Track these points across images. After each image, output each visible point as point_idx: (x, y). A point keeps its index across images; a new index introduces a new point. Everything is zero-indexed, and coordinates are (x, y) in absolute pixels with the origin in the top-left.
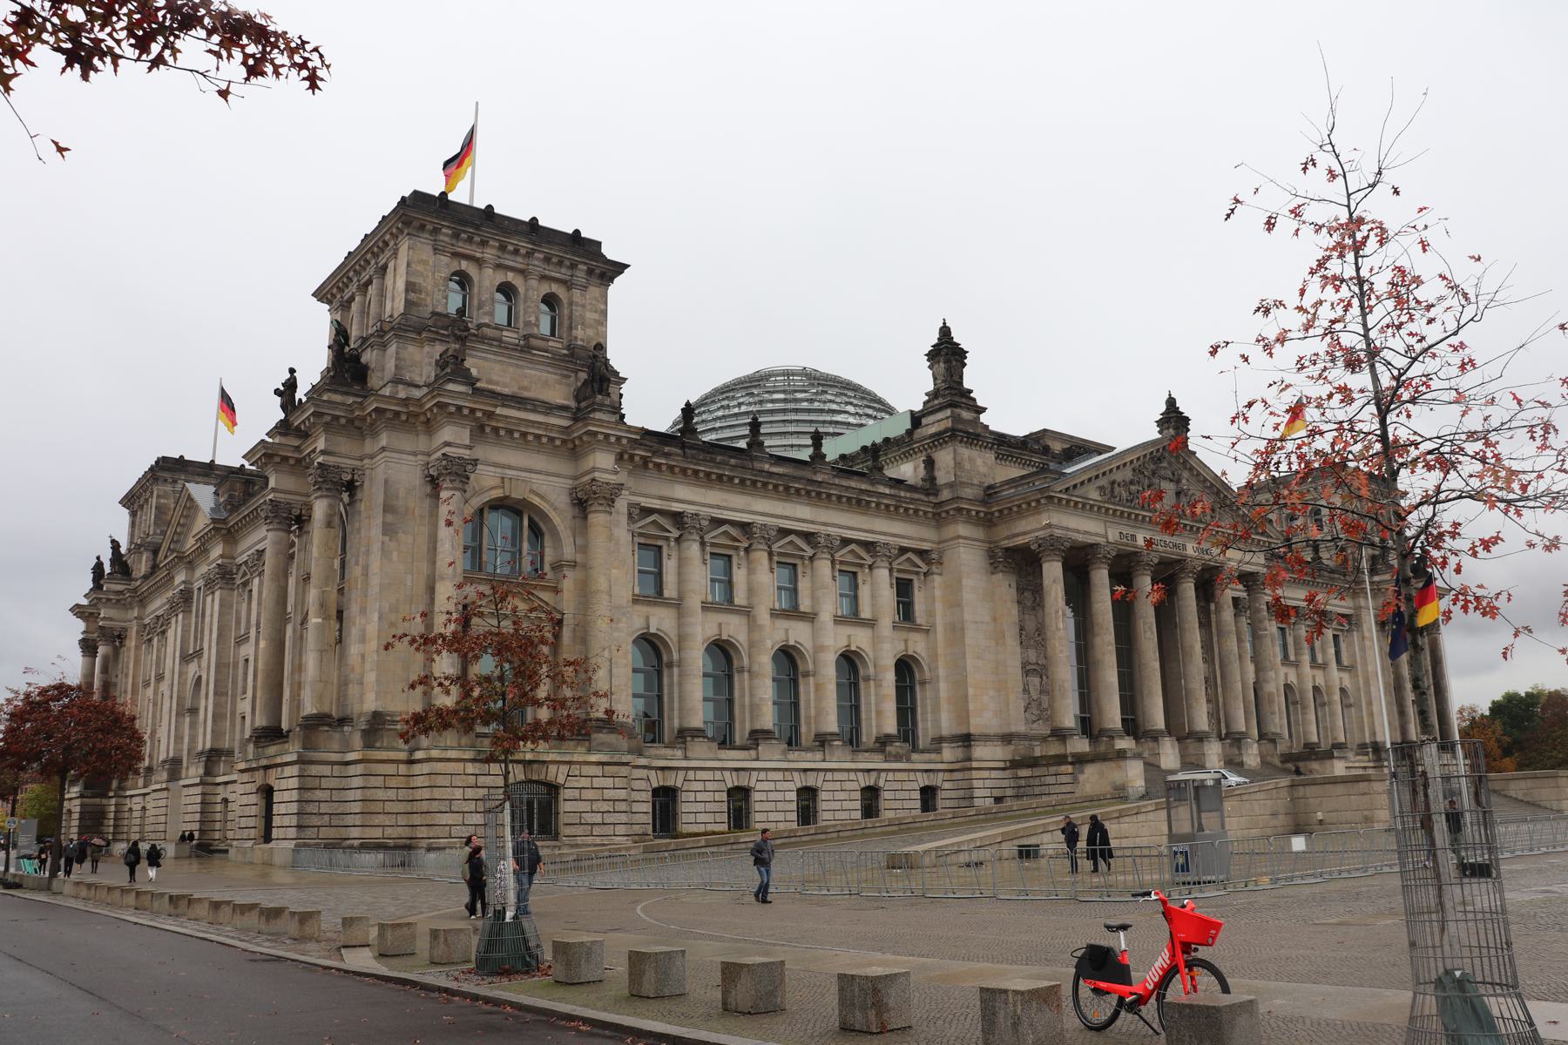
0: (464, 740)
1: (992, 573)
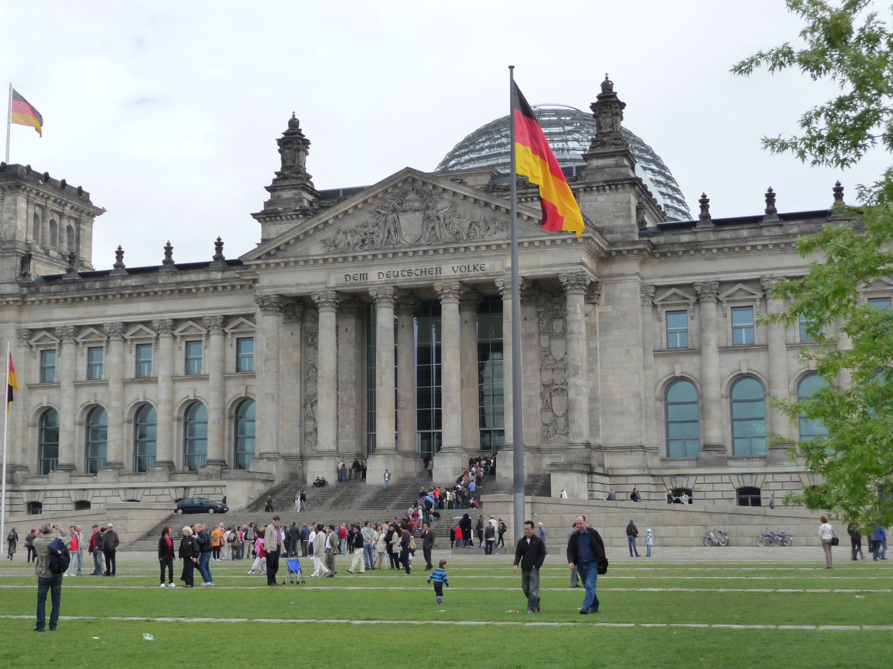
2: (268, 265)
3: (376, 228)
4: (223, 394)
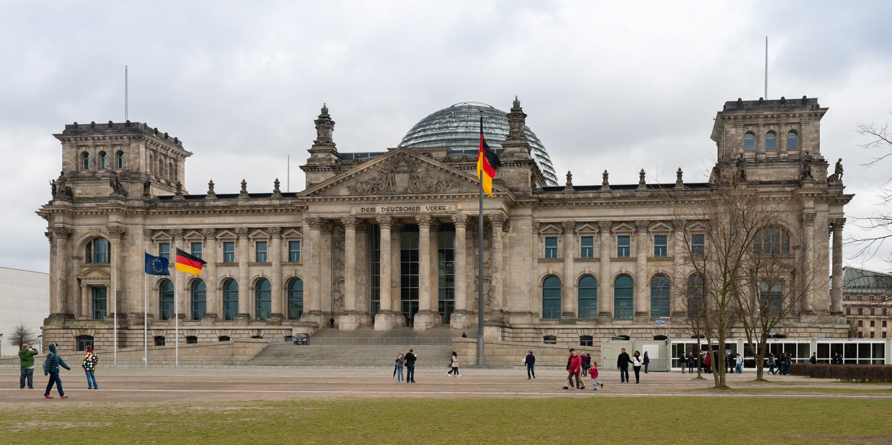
0: (60, 323)
4: (281, 275)
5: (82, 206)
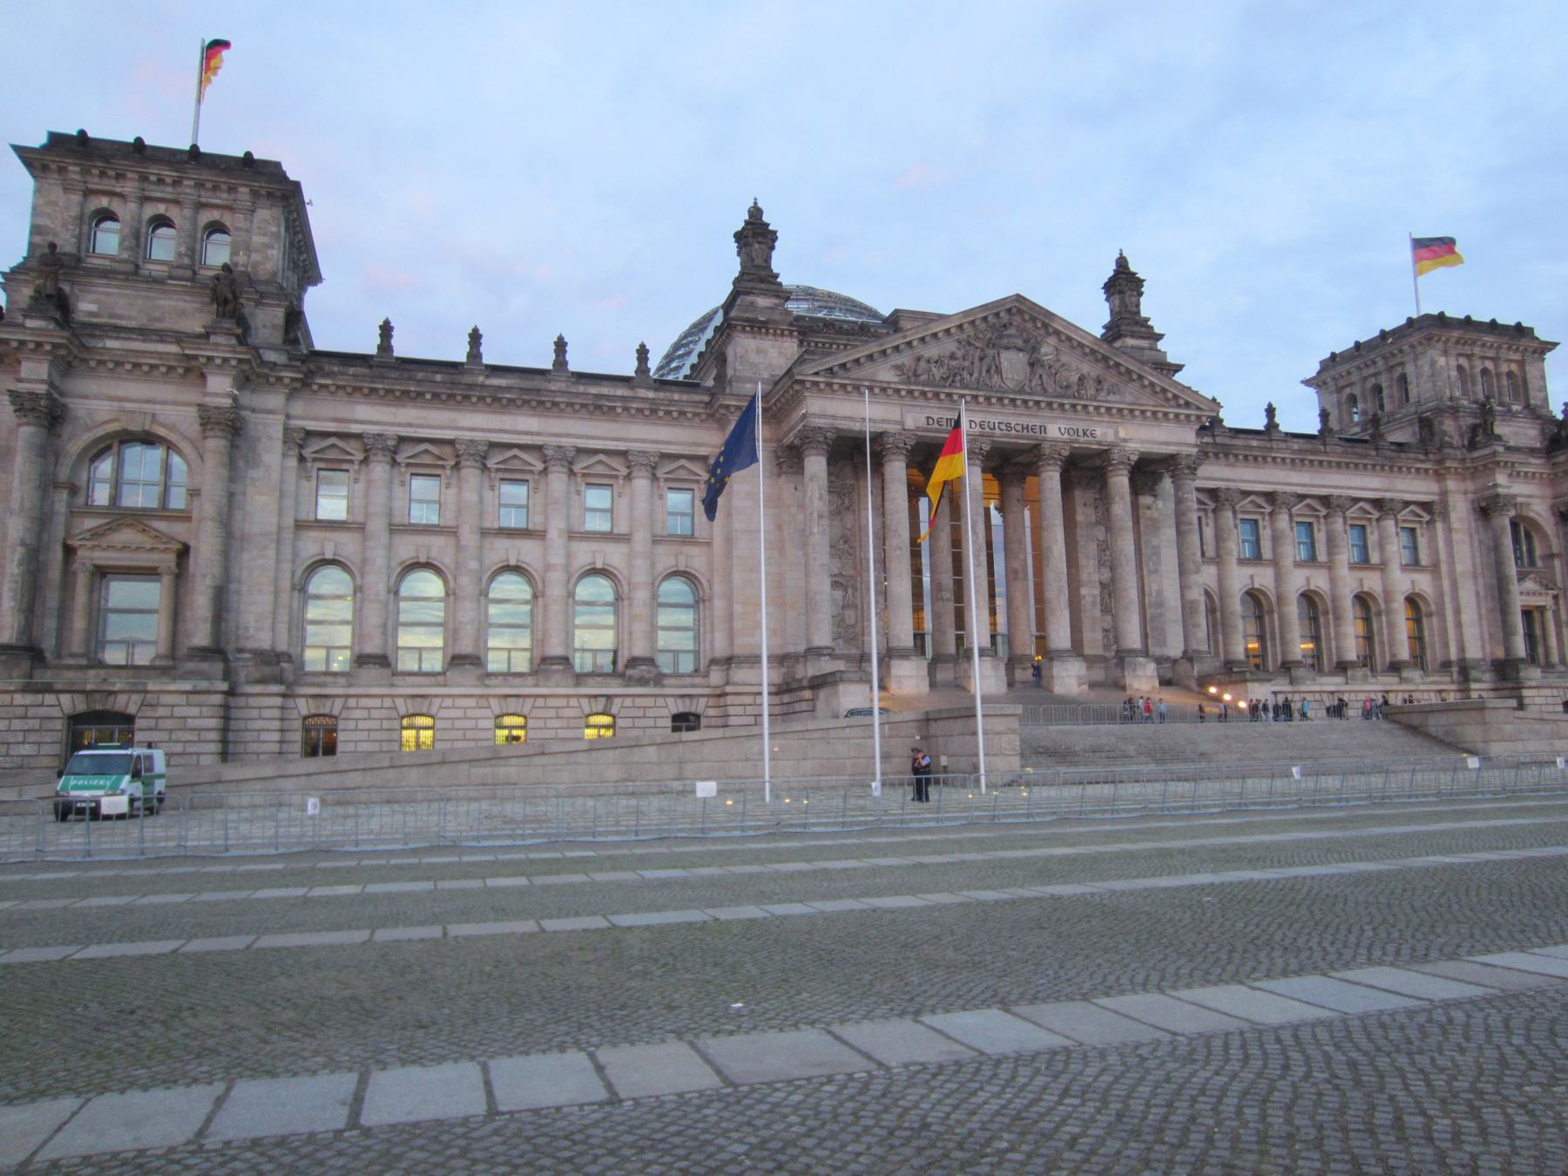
0: (15, 673)
1: (779, 476)
2: (830, 385)
3: (967, 364)
4: (653, 565)
5: (101, 345)
